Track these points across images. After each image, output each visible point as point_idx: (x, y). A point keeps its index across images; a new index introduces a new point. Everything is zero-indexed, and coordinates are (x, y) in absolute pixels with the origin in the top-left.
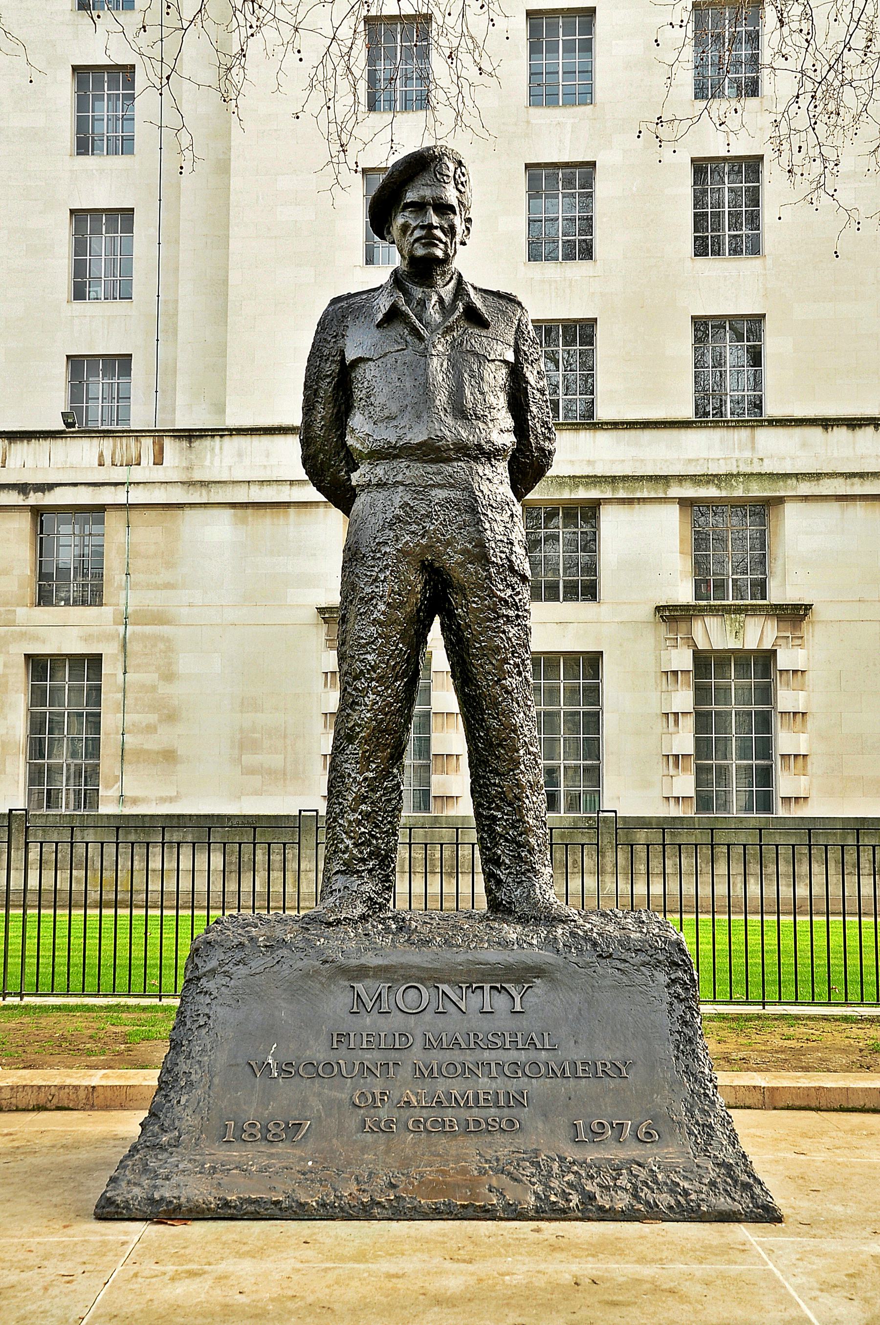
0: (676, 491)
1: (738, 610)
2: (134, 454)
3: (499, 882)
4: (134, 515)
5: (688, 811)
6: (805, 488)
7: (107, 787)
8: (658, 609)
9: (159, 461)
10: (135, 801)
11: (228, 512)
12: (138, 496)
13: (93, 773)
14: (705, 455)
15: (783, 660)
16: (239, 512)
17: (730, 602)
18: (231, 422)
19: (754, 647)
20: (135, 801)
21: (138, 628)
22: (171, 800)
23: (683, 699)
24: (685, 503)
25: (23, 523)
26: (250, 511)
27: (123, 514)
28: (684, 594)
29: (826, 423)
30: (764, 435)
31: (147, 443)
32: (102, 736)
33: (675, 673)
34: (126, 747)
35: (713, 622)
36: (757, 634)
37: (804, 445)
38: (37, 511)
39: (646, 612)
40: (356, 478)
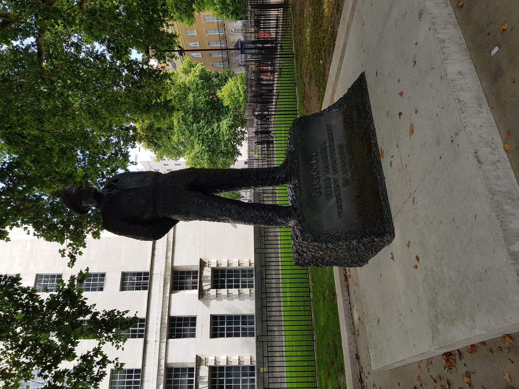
0: (168, 295)
1: (200, 277)
5: (253, 290)
6: (170, 261)
8: (199, 298)
14: (158, 287)
15: (215, 266)
17: (198, 280)
19: (210, 273)
23: (223, 292)
24: (171, 293)
28: (196, 292)
29: (153, 255)
30: (155, 271)
33: (217, 294)
35: (204, 284)
36: (207, 273)
37: (158, 261)
39: (200, 303)
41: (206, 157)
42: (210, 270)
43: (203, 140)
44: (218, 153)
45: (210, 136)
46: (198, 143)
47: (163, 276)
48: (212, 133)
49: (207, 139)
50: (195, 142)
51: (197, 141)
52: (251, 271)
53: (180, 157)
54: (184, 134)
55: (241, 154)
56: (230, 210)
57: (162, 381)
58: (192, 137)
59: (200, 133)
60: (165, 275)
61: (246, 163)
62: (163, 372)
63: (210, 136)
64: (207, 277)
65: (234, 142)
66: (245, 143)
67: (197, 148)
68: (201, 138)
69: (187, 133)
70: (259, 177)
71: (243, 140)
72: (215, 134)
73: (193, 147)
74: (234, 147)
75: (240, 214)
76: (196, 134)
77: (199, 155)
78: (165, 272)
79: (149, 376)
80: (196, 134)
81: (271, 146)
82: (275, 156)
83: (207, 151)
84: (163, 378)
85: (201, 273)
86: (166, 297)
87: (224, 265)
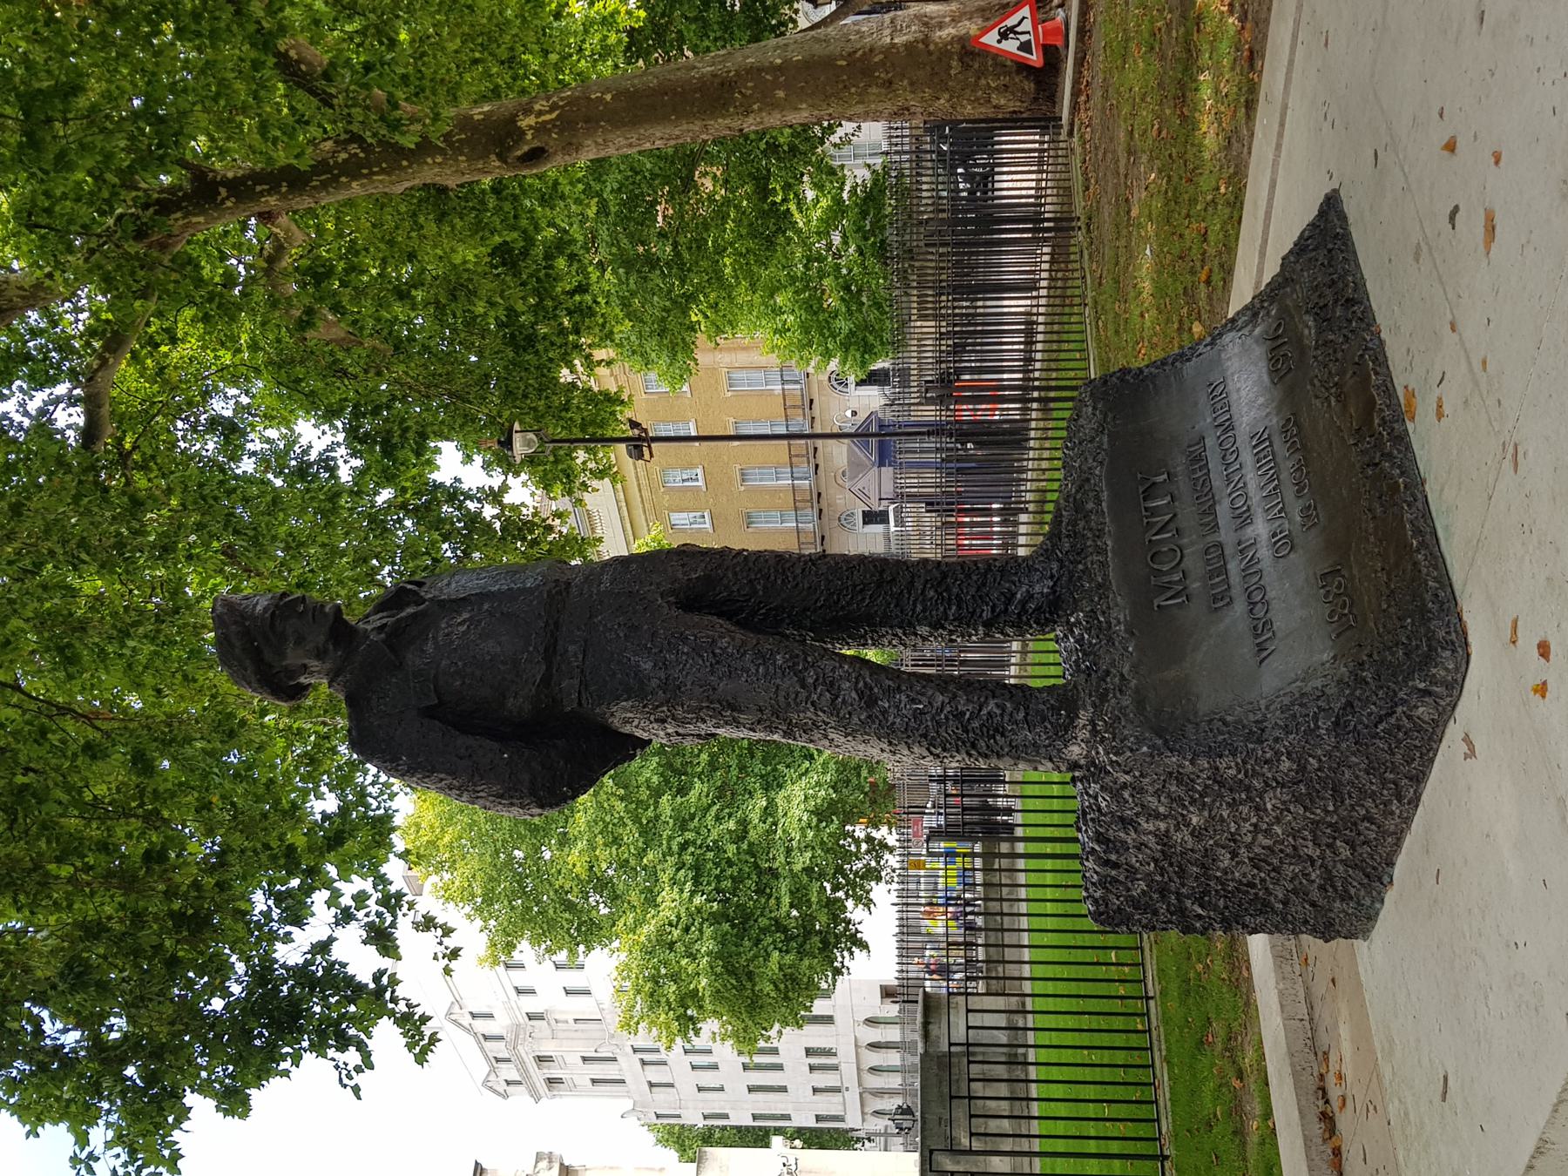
41: (708, 945)
43: (697, 868)
44: (764, 931)
45: (731, 849)
46: (674, 882)
48: (740, 835)
49: (717, 865)
50: (665, 878)
51: (670, 871)
53: (589, 949)
54: (617, 841)
55: (864, 946)
56: (832, 684)
58: (651, 856)
59: (689, 835)
61: (887, 993)
63: (731, 849)
65: (835, 889)
66: (884, 894)
67: (670, 901)
68: (688, 859)
69: (630, 834)
70: (948, 589)
71: (879, 879)
72: (751, 844)
73: (651, 900)
74: (834, 908)
75: (871, 702)
76: (670, 838)
77: (676, 933)
80: (670, 838)
81: (1005, 847)
82: (1023, 893)
83: (715, 919)
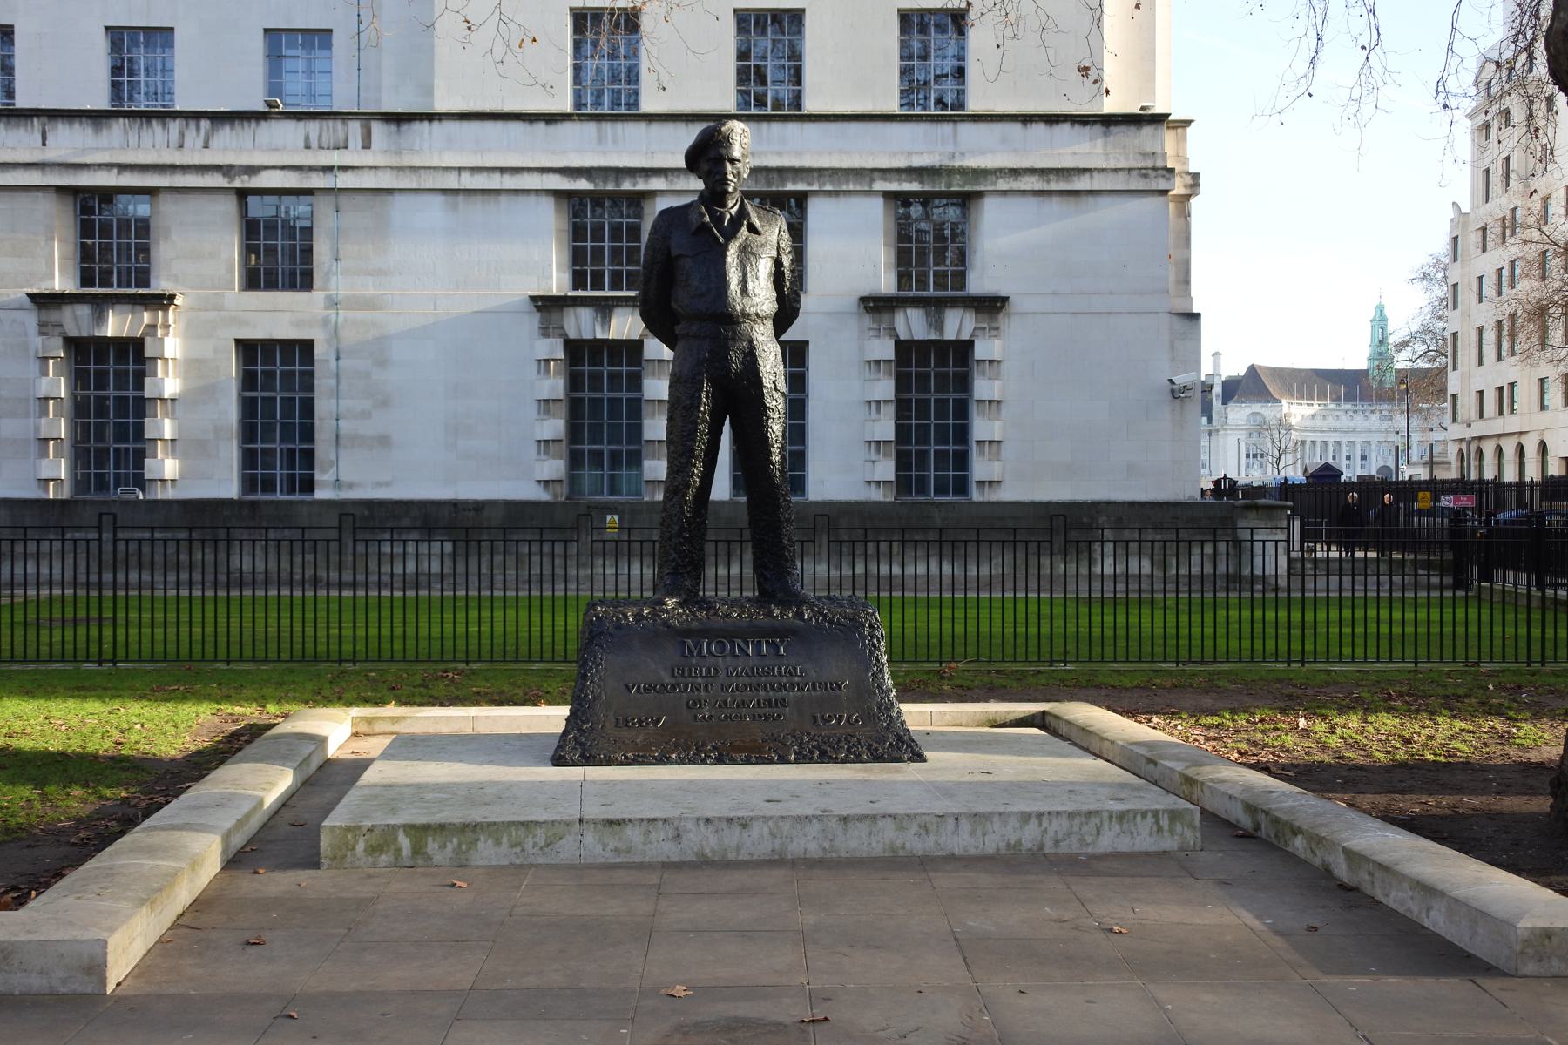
0: (879, 185)
2: (341, 136)
3: (766, 579)
4: (344, 200)
6: (1002, 185)
7: (324, 471)
8: (863, 300)
9: (367, 145)
10: (351, 486)
11: (439, 199)
12: (345, 180)
13: (309, 457)
15: (981, 350)
16: (450, 198)
18: (440, 107)
19: (953, 337)
20: (351, 486)
21: (350, 314)
22: (387, 484)
23: (885, 388)
24: (889, 196)
25: (230, 205)
26: (461, 198)
27: (331, 199)
30: (966, 129)
31: (355, 127)
32: (317, 422)
33: (878, 362)
34: (342, 432)
36: (957, 325)
37: (1004, 140)
38: (243, 194)
39: (851, 303)
40: (678, 329)
42: (965, 336)
47: (947, 162)
52: (962, 486)
57: (601, 187)
60: (950, 171)
62: (627, 185)
64: (939, 325)
78: (963, 171)
79: (615, 141)
84: (610, 187)
85: (954, 302)
86: (872, 180)
87: (983, 387)
